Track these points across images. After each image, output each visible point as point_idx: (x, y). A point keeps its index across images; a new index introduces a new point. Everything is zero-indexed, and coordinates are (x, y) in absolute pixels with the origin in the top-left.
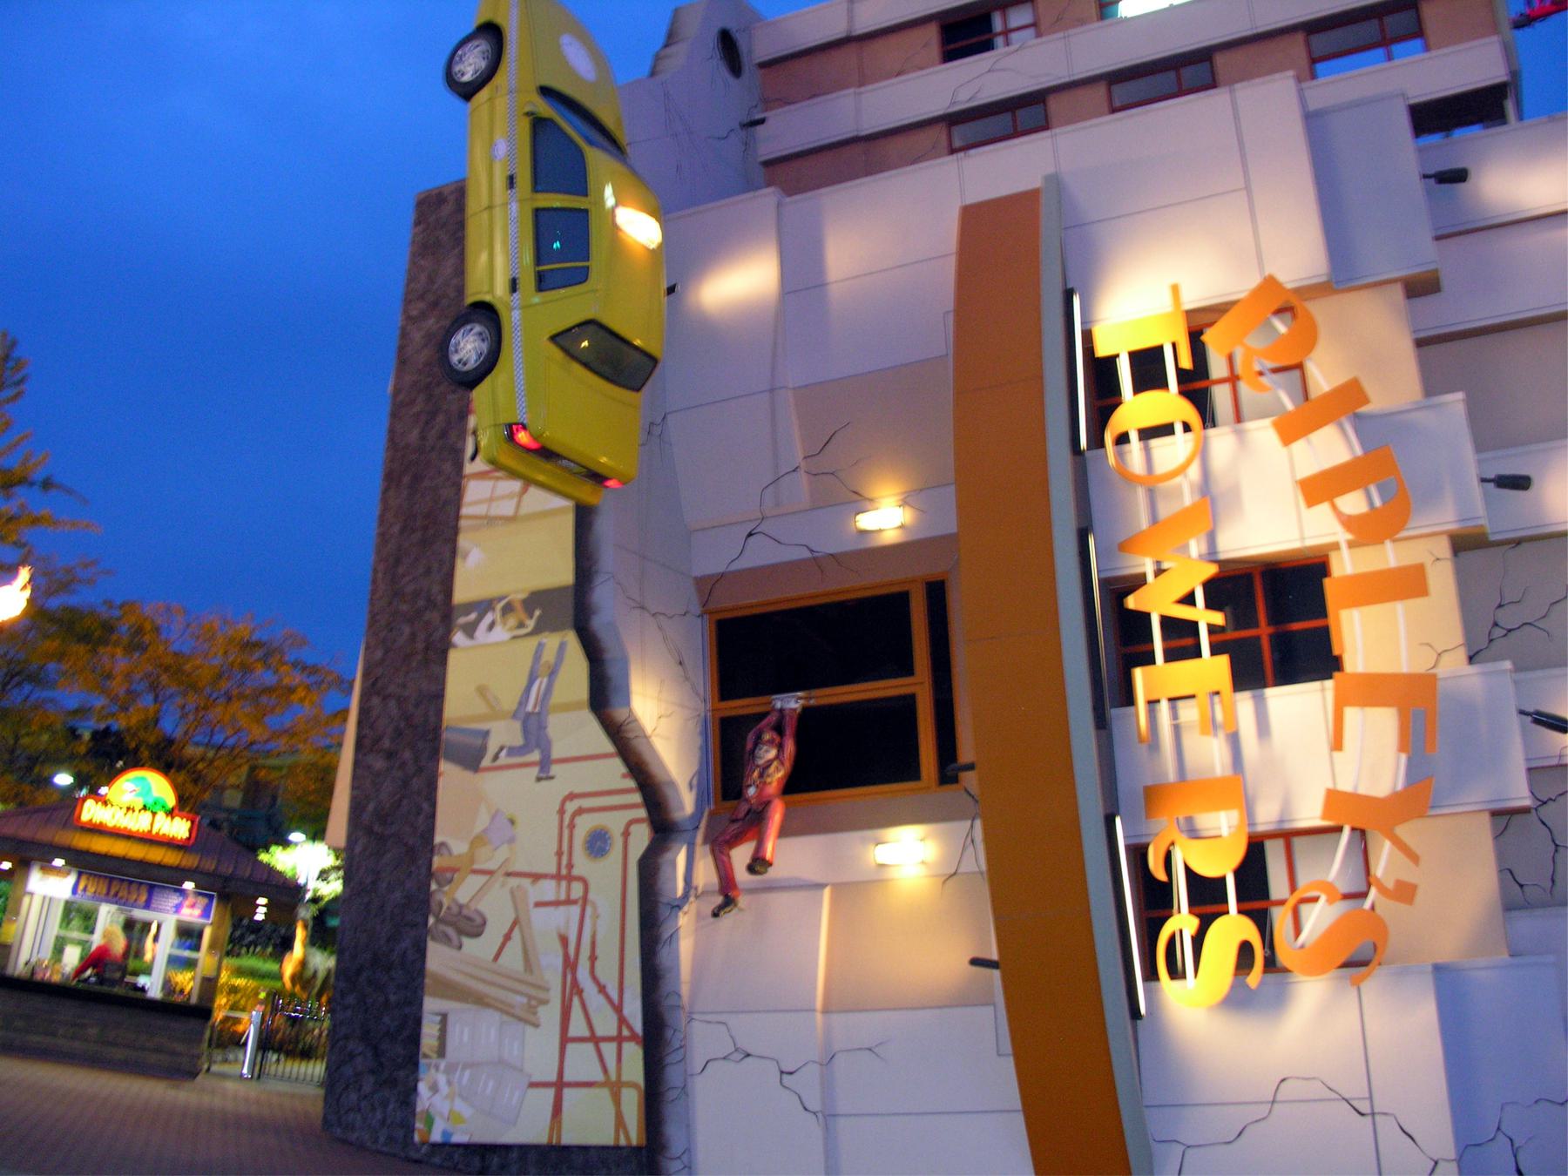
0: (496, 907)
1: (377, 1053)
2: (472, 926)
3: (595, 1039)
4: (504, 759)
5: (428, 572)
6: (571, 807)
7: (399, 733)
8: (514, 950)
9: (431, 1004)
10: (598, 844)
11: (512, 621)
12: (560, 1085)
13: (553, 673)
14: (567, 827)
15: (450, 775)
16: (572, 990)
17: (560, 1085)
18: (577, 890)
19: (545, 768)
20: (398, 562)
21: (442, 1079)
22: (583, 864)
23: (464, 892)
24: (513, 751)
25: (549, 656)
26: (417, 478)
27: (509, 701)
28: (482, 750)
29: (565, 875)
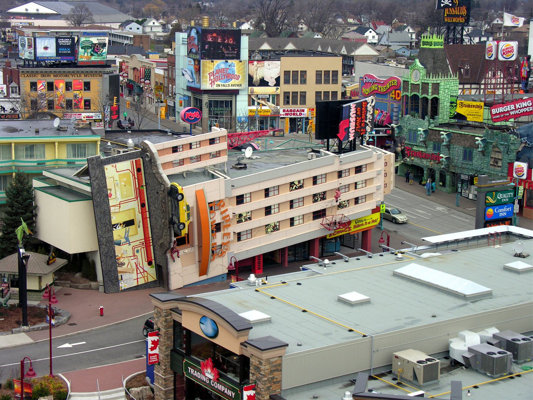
0: (126, 261)
1: (112, 282)
2: (123, 264)
3: (141, 273)
4: (124, 244)
5: (106, 220)
6: (134, 248)
7: (106, 242)
8: (129, 266)
9: (119, 274)
10: (138, 251)
11: (121, 226)
12: (137, 279)
13: (128, 232)
14: (133, 250)
15: (117, 247)
16: (137, 268)
17: (137, 279)
18: (136, 257)
19: (129, 244)
20: (101, 219)
21: (122, 282)
22: (136, 254)
23: (122, 260)
24: (125, 242)
25: (127, 230)
26: (101, 206)
27: (123, 236)
28: (121, 243)
29: (134, 256)
